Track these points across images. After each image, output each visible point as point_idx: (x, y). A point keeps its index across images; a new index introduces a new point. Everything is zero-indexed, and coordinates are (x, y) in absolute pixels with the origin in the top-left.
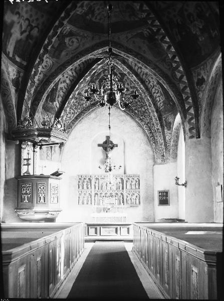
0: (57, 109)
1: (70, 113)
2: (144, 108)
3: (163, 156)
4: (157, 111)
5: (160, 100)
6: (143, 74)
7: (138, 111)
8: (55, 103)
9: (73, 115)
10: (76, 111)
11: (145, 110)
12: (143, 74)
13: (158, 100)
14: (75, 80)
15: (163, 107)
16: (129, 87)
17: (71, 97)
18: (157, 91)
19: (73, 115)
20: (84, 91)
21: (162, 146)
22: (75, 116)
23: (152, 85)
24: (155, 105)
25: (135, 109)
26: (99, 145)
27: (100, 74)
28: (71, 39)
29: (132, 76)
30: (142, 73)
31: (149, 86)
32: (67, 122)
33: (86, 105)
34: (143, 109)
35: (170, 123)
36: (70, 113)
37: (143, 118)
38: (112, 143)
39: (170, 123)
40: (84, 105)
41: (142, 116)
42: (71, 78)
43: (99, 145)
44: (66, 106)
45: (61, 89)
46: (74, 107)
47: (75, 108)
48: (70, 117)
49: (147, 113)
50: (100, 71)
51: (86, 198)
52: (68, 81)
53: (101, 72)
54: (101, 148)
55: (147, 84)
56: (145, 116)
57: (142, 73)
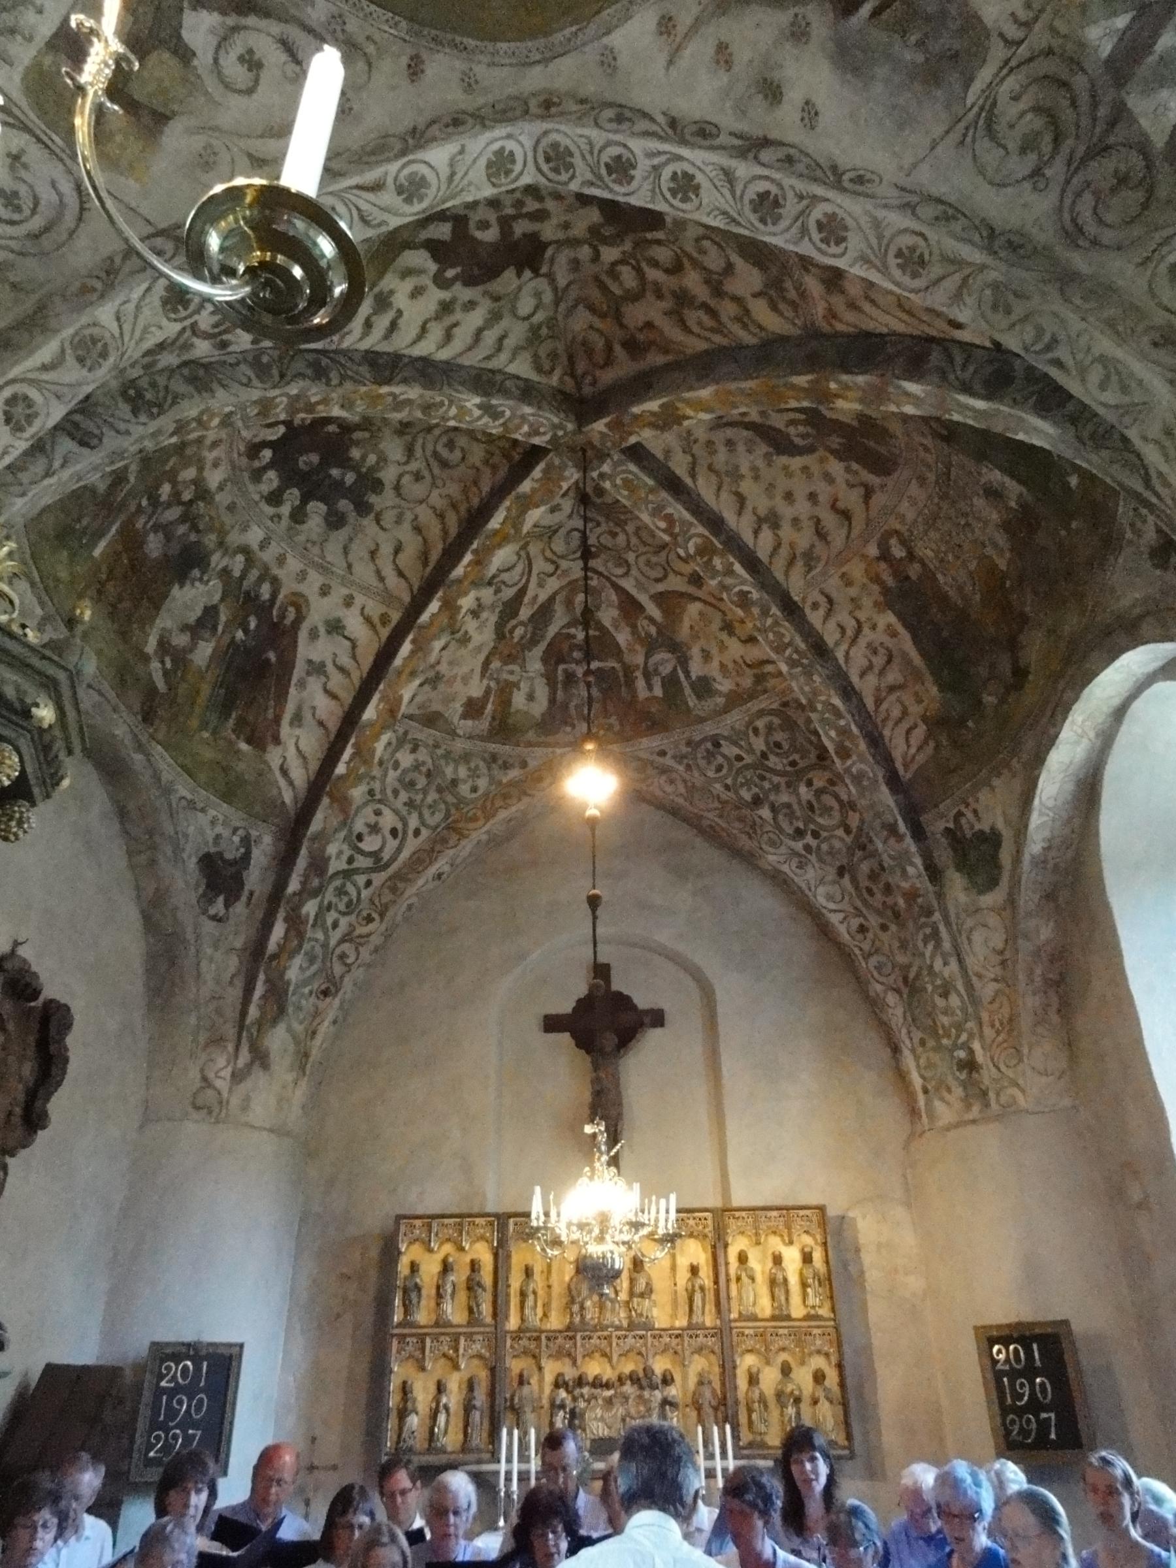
0: (288, 797)
1: (374, 829)
2: (809, 783)
3: (970, 1065)
4: (893, 781)
5: (905, 713)
6: (791, 562)
7: (774, 809)
8: (274, 757)
9: (392, 844)
10: (413, 822)
11: (819, 793)
12: (791, 562)
13: (896, 713)
14: (396, 616)
15: (930, 749)
16: (713, 670)
17: (370, 713)
18: (879, 661)
19: (392, 844)
20: (458, 707)
21: (954, 1000)
22: (405, 854)
23: (851, 625)
24: (875, 741)
25: (757, 802)
26: (552, 1024)
27: (544, 613)
28: (235, 29)
29: (729, 572)
30: (784, 552)
31: (830, 636)
32: (361, 880)
33: (474, 789)
34: (803, 789)
35: (993, 840)
36: (374, 829)
37: (807, 848)
38: (623, 1002)
39: (993, 840)
40: (464, 789)
41: (799, 833)
42: (375, 609)
43: (552, 1024)
44: (341, 769)
45: (317, 669)
46: (404, 796)
47: (410, 804)
48: (376, 855)
49: (827, 810)
50: (543, 597)
51: (453, 1398)
52: (354, 624)
53: (552, 599)
54: (565, 1038)
55: (815, 618)
56: (815, 835)
57: (784, 552)
